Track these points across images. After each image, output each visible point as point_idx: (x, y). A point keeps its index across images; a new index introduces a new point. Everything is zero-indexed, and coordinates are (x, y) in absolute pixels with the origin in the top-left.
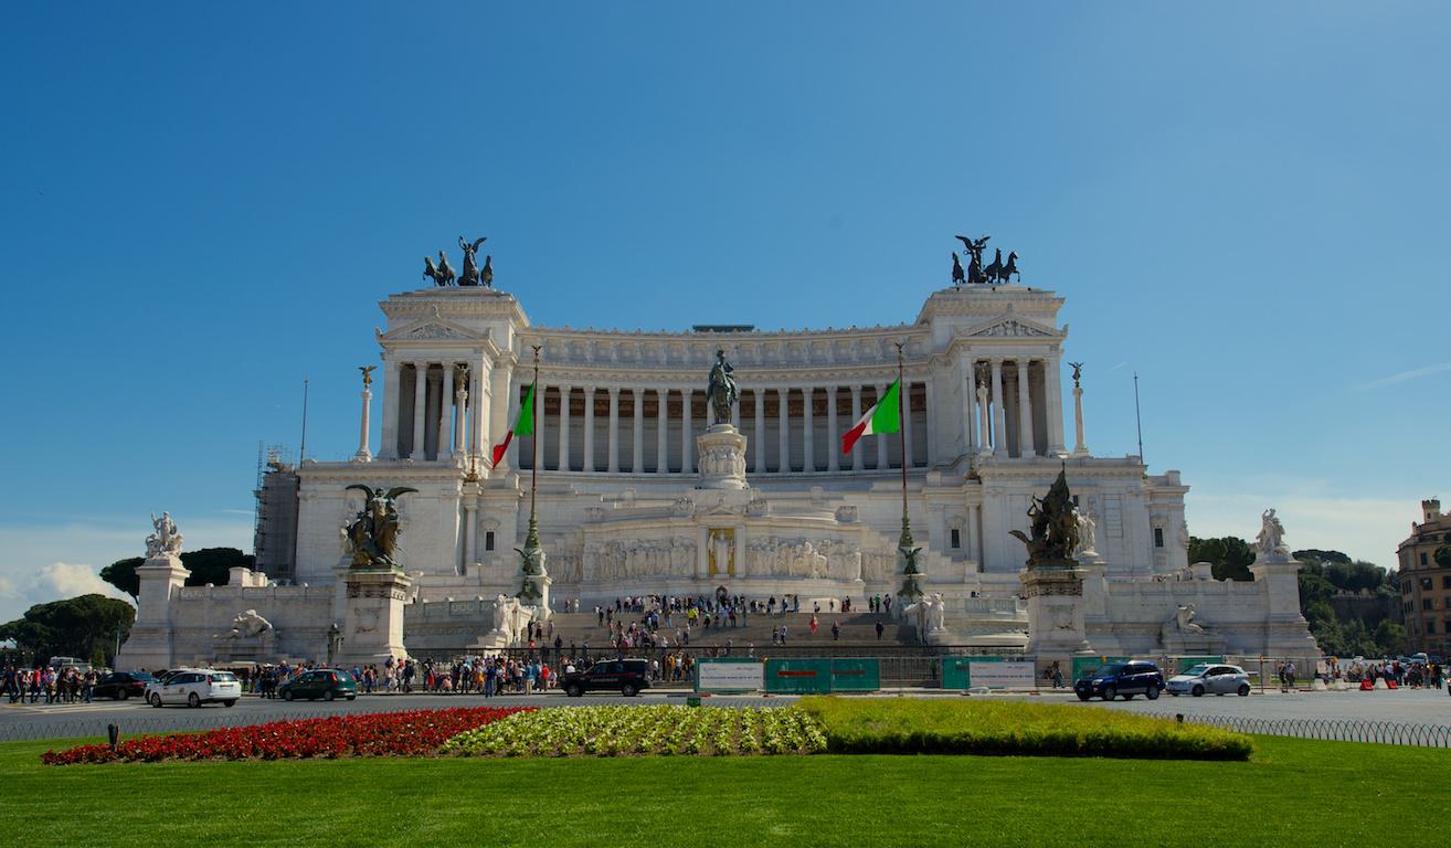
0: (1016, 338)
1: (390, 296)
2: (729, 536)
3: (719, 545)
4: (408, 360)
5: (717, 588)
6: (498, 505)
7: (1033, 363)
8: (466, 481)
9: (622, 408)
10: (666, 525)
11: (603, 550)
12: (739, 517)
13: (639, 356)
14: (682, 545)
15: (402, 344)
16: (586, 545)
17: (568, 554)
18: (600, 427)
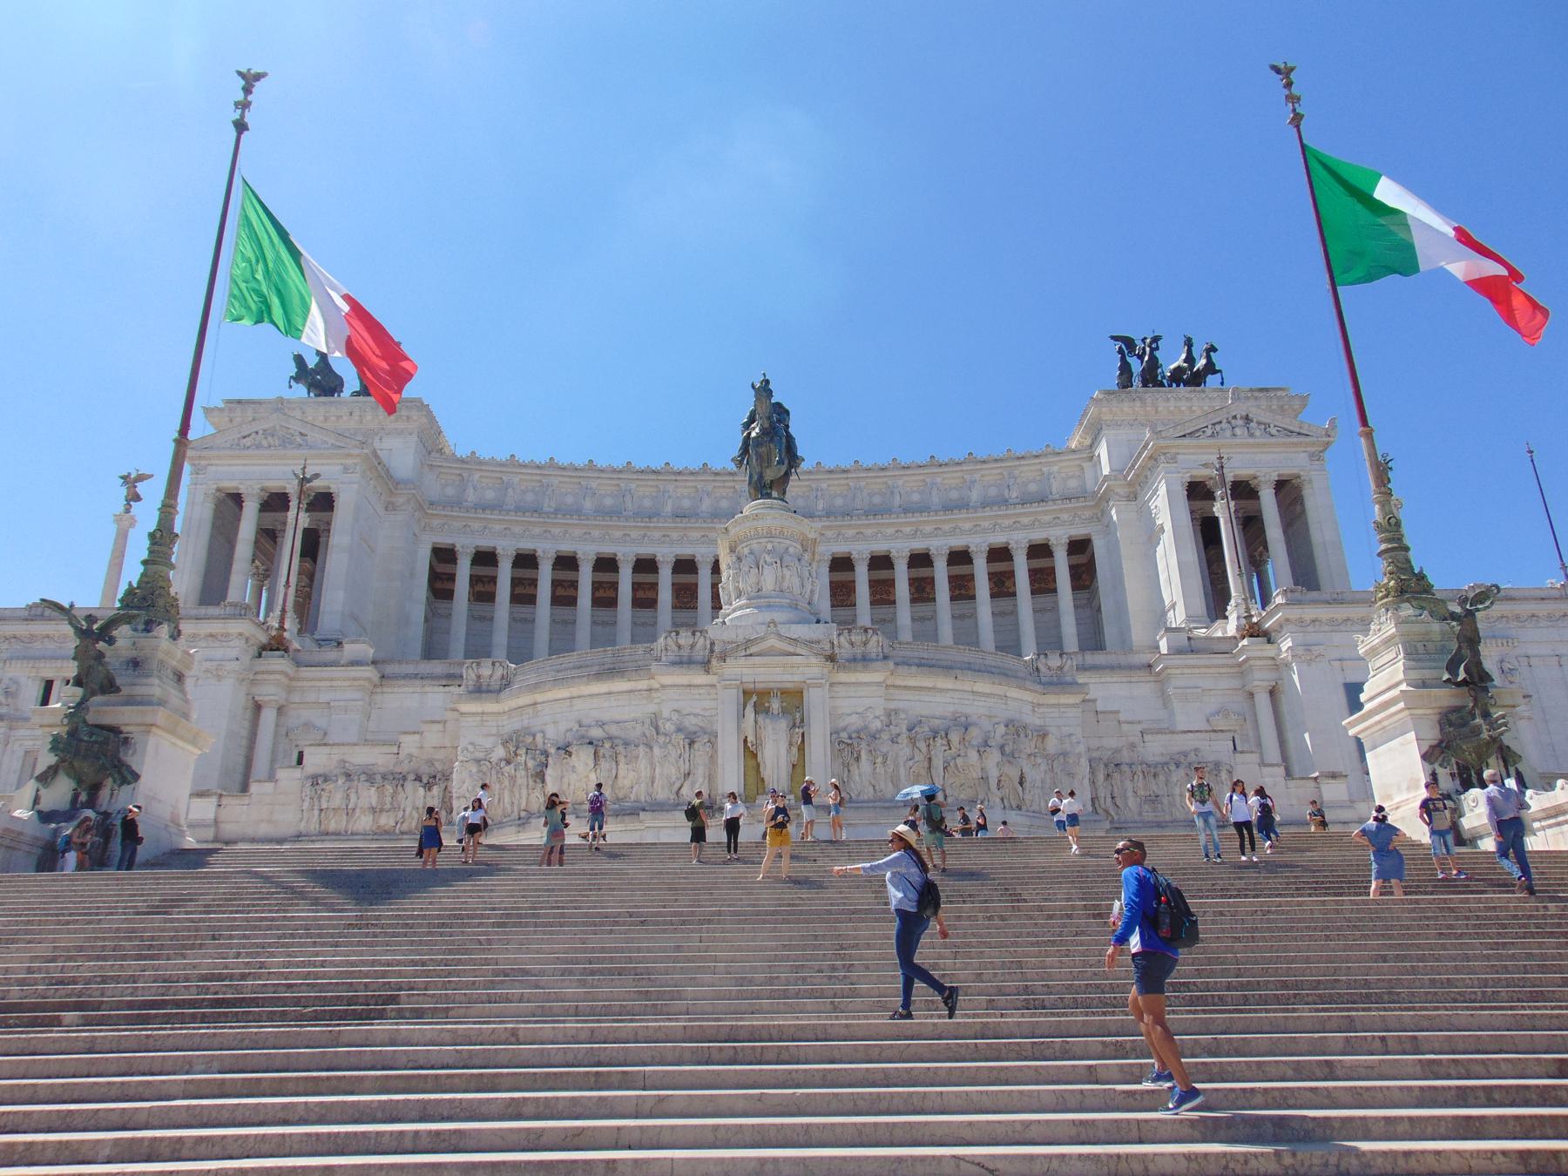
0: (1251, 440)
1: (229, 402)
2: (793, 701)
4: (230, 485)
6: (324, 698)
7: (1281, 485)
8: (264, 648)
9: (600, 594)
11: (500, 752)
12: (813, 660)
13: (629, 504)
14: (679, 730)
15: (219, 458)
16: (463, 743)
17: (425, 771)
18: (565, 623)
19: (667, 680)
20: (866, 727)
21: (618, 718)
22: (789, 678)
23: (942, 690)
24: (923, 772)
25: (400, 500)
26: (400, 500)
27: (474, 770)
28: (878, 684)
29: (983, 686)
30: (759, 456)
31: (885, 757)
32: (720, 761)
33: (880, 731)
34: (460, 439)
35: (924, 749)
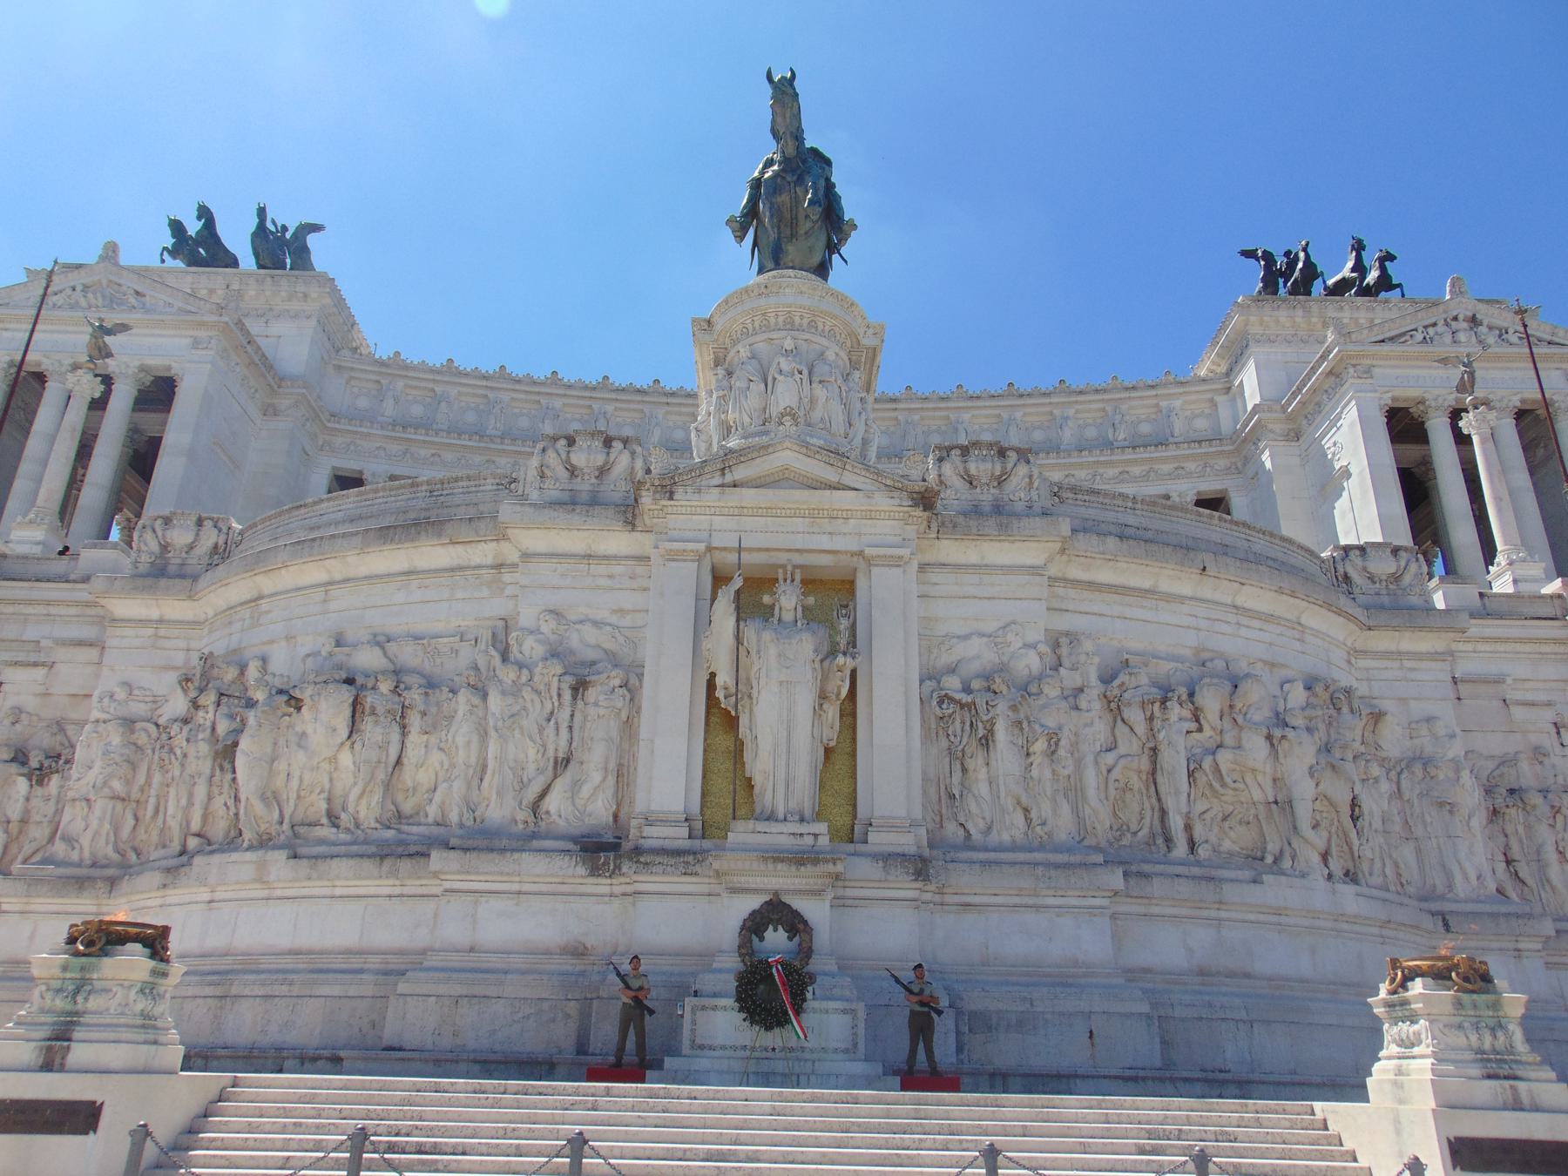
3: (767, 636)
5: (754, 902)
10: (483, 553)
12: (883, 502)
14: (554, 654)
19: (536, 540)
20: (1002, 668)
21: (421, 627)
22: (824, 542)
23: (1170, 598)
24: (1136, 783)
25: (284, 403)
26: (284, 403)
27: (116, 740)
28: (1034, 570)
29: (1258, 597)
30: (776, 212)
31: (1053, 738)
32: (644, 733)
33: (1040, 678)
34: (380, 334)
35: (1141, 728)
